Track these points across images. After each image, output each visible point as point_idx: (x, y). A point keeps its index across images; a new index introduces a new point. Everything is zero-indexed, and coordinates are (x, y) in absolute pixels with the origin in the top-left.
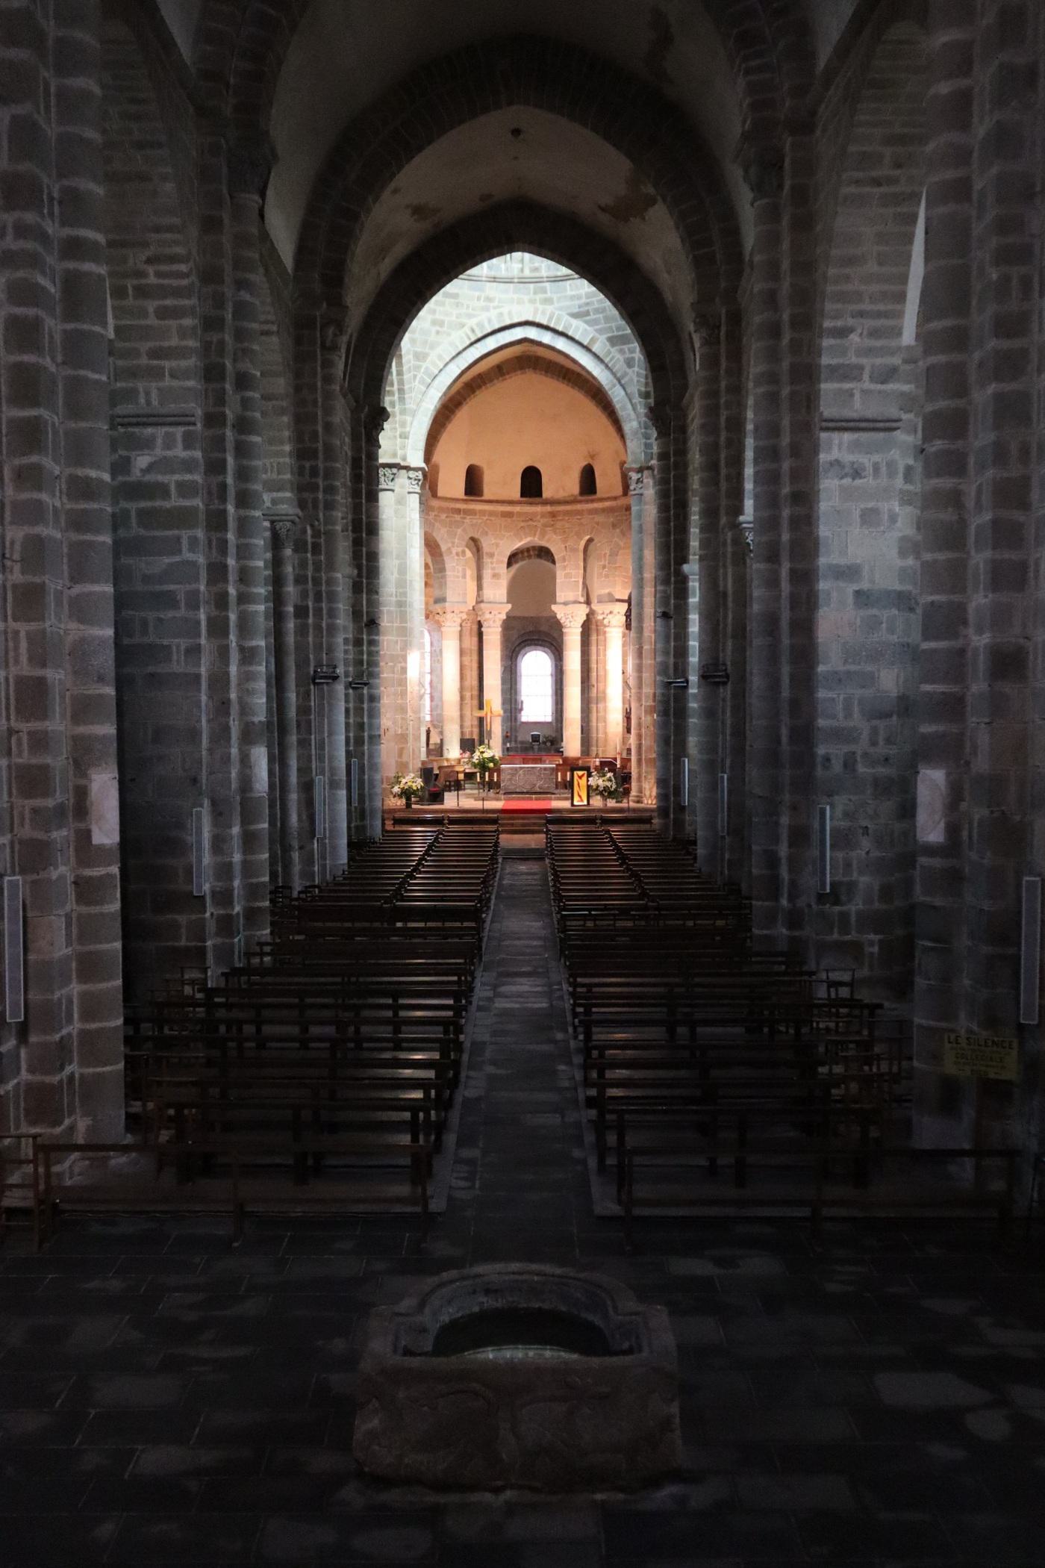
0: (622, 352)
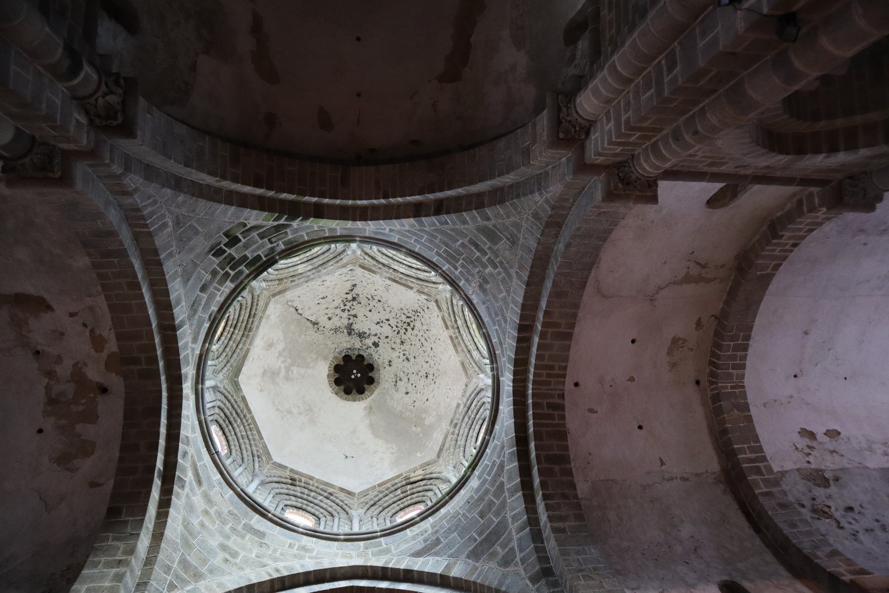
0: (493, 555)
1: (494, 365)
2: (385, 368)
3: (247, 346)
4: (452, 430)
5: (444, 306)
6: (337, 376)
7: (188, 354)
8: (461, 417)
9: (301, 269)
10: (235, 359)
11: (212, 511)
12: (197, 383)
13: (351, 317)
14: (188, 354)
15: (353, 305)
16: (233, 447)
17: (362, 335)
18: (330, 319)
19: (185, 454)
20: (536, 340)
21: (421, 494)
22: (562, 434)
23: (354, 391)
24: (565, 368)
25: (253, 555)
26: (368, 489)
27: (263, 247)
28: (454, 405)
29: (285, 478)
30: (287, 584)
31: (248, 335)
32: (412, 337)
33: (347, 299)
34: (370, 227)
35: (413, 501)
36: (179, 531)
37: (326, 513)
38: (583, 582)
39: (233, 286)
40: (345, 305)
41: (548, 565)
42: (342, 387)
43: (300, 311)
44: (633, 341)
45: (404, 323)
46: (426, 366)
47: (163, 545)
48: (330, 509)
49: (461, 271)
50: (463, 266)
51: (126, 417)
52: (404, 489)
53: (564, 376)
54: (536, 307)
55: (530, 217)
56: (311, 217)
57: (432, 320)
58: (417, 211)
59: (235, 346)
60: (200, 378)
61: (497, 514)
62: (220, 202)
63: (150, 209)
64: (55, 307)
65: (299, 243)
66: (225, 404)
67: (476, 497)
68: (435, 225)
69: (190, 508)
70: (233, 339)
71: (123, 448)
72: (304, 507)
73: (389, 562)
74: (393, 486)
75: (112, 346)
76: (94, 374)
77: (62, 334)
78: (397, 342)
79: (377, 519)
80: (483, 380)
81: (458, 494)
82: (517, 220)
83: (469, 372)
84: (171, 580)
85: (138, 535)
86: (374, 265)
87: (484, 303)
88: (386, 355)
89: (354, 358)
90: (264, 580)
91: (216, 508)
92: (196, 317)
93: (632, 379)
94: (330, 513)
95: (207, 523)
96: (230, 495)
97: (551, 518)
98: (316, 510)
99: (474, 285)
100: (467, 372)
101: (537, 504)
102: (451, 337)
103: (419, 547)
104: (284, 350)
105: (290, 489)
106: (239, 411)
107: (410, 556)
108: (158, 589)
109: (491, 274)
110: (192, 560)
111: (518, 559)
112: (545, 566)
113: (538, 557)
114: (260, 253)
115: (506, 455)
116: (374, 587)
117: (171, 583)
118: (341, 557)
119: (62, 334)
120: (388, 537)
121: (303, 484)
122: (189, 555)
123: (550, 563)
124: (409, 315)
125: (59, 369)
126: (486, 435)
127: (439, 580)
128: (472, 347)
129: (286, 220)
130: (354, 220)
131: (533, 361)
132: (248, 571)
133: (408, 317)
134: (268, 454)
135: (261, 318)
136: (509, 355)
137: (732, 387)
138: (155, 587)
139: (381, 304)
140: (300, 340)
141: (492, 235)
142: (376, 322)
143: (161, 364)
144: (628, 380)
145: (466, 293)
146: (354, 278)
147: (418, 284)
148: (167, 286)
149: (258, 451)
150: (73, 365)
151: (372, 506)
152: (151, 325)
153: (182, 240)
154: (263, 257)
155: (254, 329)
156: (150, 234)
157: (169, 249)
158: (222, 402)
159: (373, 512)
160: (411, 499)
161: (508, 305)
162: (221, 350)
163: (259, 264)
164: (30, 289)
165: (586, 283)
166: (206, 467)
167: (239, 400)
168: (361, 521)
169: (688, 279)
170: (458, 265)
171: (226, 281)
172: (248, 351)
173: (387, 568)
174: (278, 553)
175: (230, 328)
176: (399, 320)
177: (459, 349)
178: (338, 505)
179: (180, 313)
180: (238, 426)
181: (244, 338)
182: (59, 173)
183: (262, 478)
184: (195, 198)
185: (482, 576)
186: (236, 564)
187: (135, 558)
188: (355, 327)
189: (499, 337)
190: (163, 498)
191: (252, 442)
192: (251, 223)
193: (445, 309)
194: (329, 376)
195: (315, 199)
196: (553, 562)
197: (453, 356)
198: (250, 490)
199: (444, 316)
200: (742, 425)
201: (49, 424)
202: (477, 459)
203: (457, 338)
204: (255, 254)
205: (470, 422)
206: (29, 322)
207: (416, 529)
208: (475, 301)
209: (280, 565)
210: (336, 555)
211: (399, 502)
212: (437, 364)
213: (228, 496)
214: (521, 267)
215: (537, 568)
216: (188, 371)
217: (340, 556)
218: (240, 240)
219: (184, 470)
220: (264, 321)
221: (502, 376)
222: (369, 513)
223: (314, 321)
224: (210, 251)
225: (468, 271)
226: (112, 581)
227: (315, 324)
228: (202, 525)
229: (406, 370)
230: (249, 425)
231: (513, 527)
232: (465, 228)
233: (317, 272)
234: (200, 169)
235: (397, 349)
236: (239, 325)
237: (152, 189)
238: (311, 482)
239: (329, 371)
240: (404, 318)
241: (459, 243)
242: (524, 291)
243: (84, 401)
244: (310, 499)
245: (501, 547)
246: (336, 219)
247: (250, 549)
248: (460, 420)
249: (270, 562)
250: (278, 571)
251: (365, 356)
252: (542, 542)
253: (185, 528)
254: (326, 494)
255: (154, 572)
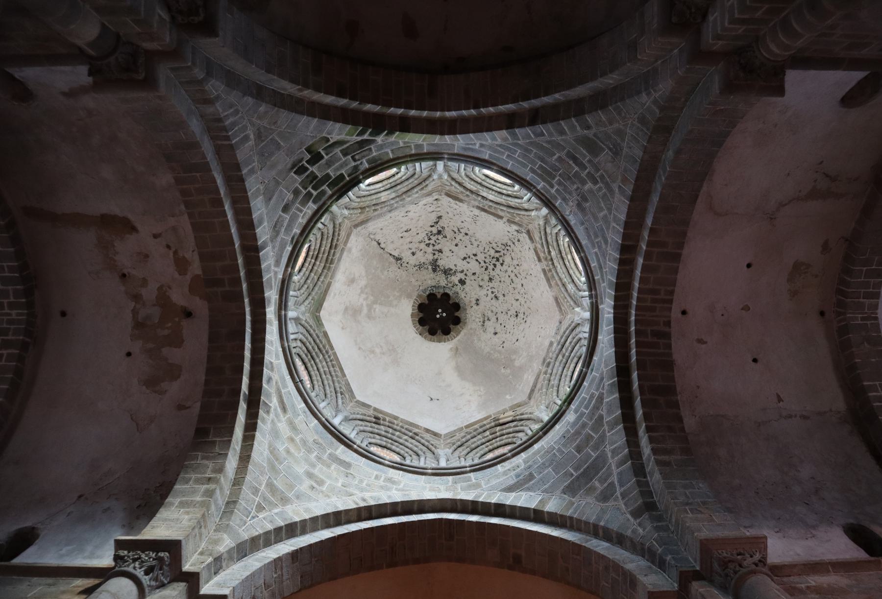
0: (592, 489)
1: (593, 292)
2: (472, 307)
3: (329, 279)
4: (544, 370)
5: (537, 237)
6: (421, 315)
7: (270, 277)
8: (555, 356)
9: (384, 196)
10: (317, 293)
11: (297, 439)
12: (280, 309)
13: (436, 253)
14: (270, 277)
15: (438, 239)
16: (315, 382)
17: (447, 272)
18: (413, 254)
19: (270, 379)
20: (640, 261)
21: (511, 435)
22: (668, 365)
23: (439, 332)
24: (672, 293)
25: (339, 485)
26: (455, 431)
27: (347, 165)
28: (547, 343)
29: (368, 416)
30: (374, 514)
31: (329, 267)
32: (502, 274)
33: (431, 232)
34: (458, 142)
35: (503, 442)
36: (265, 455)
37: (411, 453)
38: (690, 515)
39: (315, 207)
40: (430, 239)
41: (651, 500)
42: (427, 327)
43: (382, 245)
44: (749, 266)
45: (493, 258)
46: (516, 304)
47: (250, 467)
48: (415, 449)
49: (557, 189)
50: (560, 183)
51: (211, 340)
52: (493, 430)
53: (671, 301)
54: (641, 225)
55: (635, 123)
56: (397, 131)
57: (523, 253)
58: (510, 122)
59: (316, 278)
60: (282, 305)
61: (595, 448)
62: (302, 113)
63: (231, 120)
64: (139, 229)
65: (383, 161)
66: (307, 338)
67: (572, 432)
68: (529, 137)
69: (276, 434)
70: (314, 271)
71: (209, 371)
72: (389, 445)
73: (480, 497)
74: (481, 427)
75: (196, 268)
76: (179, 297)
77: (147, 256)
78: (485, 279)
79: (465, 460)
80: (579, 314)
81: (553, 429)
82: (621, 127)
83: (563, 308)
84: (259, 501)
85: (226, 455)
86: (462, 192)
87: (582, 224)
88: (473, 293)
89: (439, 296)
90: (350, 508)
91: (301, 436)
92: (279, 239)
93: (746, 308)
94: (415, 452)
95: (292, 450)
96: (315, 425)
97: (654, 451)
98: (401, 449)
99: (571, 204)
100: (560, 308)
101: (639, 438)
102: (544, 271)
103: (511, 482)
104: (366, 286)
105: (374, 428)
106: (321, 346)
107: (501, 491)
108: (247, 509)
109: (590, 191)
110: (279, 484)
111: (618, 493)
112: (649, 500)
113: (640, 491)
114: (343, 172)
115: (606, 387)
116: (464, 520)
117: (259, 505)
118: (429, 490)
119: (147, 256)
120: (478, 472)
121: (387, 424)
122: (276, 479)
123: (653, 498)
124: (498, 249)
125: (143, 292)
126: (583, 368)
127: (532, 515)
128: (566, 280)
129: (370, 135)
130: (442, 133)
131: (636, 284)
132: (334, 499)
133: (497, 252)
134: (351, 391)
135: (343, 250)
136: (609, 279)
137: (863, 319)
138: (244, 506)
139: (468, 237)
140: (383, 277)
141: (592, 147)
142: (462, 258)
143: (244, 286)
144: (742, 309)
145: (563, 213)
146: (438, 209)
147: (508, 212)
148: (249, 203)
149: (340, 388)
150: (158, 288)
151: (459, 447)
152: (234, 245)
153: (264, 155)
154: (346, 176)
155: (336, 261)
156: (232, 147)
157: (250, 164)
158: (304, 335)
159: (460, 453)
160: (500, 441)
161: (609, 225)
162: (302, 281)
163: (342, 184)
164: (114, 208)
165: (697, 197)
166: (290, 394)
167: (321, 335)
168: (448, 460)
169: (814, 194)
170: (554, 182)
171: (308, 202)
172: (329, 285)
173: (477, 502)
174: (364, 484)
175: (312, 258)
176: (487, 255)
177: (553, 283)
178: (423, 445)
179: (263, 233)
180: (320, 361)
181: (326, 271)
182: (143, 75)
183: (346, 414)
184: (276, 108)
185: (578, 511)
186: (322, 492)
187: (224, 477)
188: (440, 263)
189: (598, 261)
190: (249, 421)
191: (335, 378)
192: (334, 138)
193: (538, 239)
194: (412, 315)
195: (400, 111)
196: (656, 497)
197: (545, 292)
198: (336, 421)
199: (536, 248)
200: (873, 360)
201: (136, 347)
202: (574, 392)
203: (550, 270)
204: (338, 173)
205: (564, 360)
206: (116, 244)
207: (507, 465)
208: (572, 221)
209: (367, 495)
210: (424, 488)
211: (487, 443)
212: (528, 302)
213: (312, 425)
214: (625, 180)
215: (640, 501)
216: (272, 295)
217: (428, 489)
218: (322, 157)
219: (269, 396)
220: (345, 254)
221: (602, 303)
222: (457, 453)
223: (396, 255)
224: (292, 168)
225: (566, 188)
226: (203, 496)
227: (398, 259)
228: (288, 452)
229: (494, 309)
230: (331, 361)
231: (613, 462)
232: (563, 140)
233: (401, 200)
234: (282, 76)
235: (485, 287)
236: (320, 256)
237: (233, 97)
238: (395, 422)
239: (413, 310)
240: (492, 252)
241: (555, 157)
242: (627, 207)
243: (170, 325)
244: (395, 438)
245: (600, 482)
246: (423, 133)
247: (336, 478)
248: (554, 358)
249: (356, 492)
250: (364, 500)
251: (451, 294)
252: (645, 477)
253: (271, 453)
254: (411, 434)
255: (242, 492)
